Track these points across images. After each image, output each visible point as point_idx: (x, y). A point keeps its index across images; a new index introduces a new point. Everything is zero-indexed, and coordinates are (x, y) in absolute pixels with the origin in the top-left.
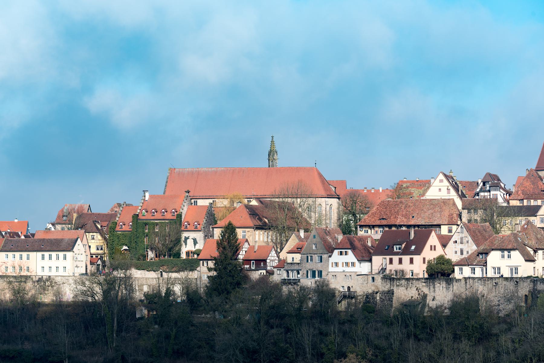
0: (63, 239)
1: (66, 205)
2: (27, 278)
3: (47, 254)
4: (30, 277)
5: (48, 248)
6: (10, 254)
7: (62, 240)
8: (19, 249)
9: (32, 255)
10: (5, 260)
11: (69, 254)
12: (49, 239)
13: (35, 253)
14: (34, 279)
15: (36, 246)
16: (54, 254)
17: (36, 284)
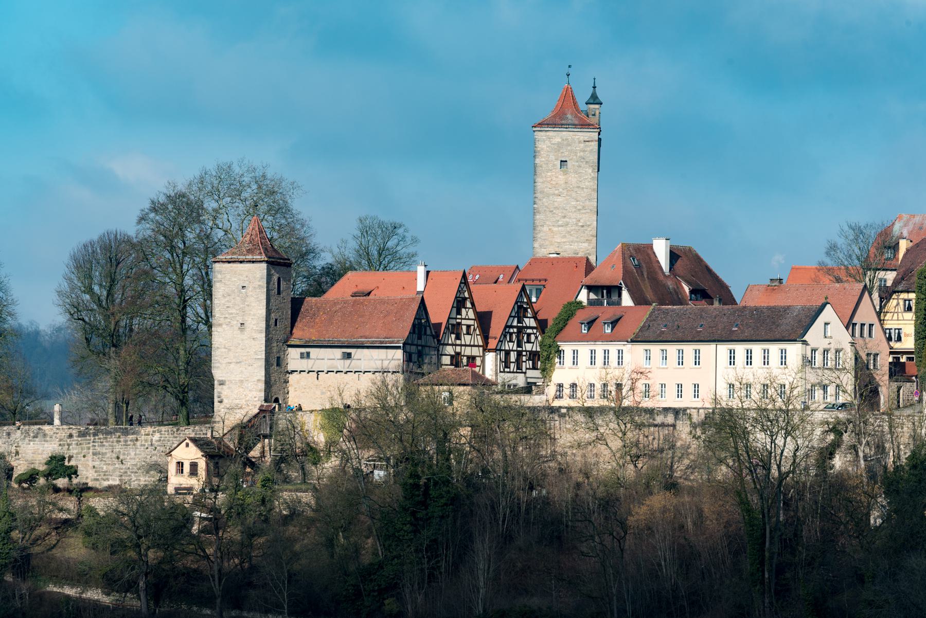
0: (789, 307)
1: (900, 218)
2: (677, 412)
3: (740, 349)
4: (685, 410)
5: (747, 334)
6: (655, 349)
7: (787, 309)
8: (680, 335)
9: (707, 350)
10: (643, 364)
11: (794, 351)
12: (756, 309)
13: (712, 346)
14: (695, 419)
15: (720, 326)
16: (757, 349)
17: (699, 432)
